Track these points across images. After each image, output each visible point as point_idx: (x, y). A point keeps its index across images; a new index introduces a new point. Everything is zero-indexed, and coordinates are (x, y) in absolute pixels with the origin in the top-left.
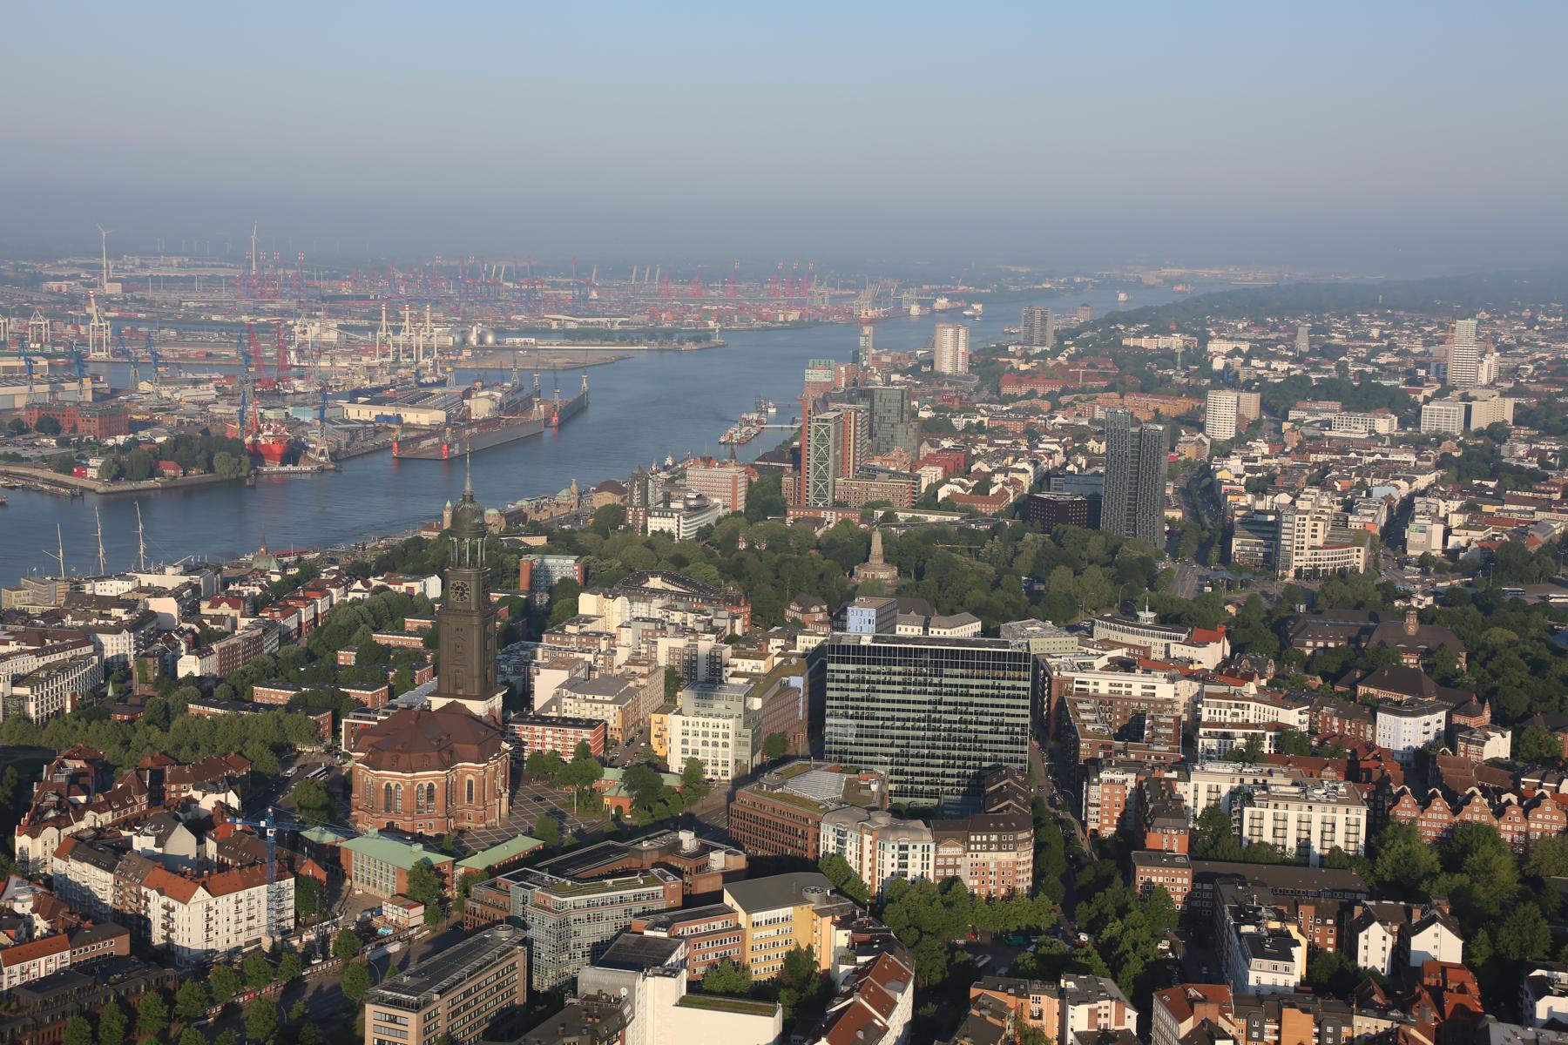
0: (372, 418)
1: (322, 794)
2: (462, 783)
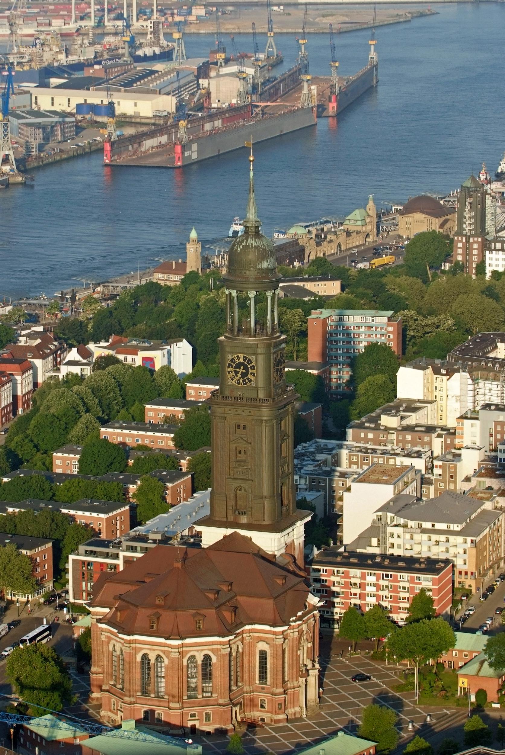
0: (72, 109)
1: (52, 668)
2: (251, 654)
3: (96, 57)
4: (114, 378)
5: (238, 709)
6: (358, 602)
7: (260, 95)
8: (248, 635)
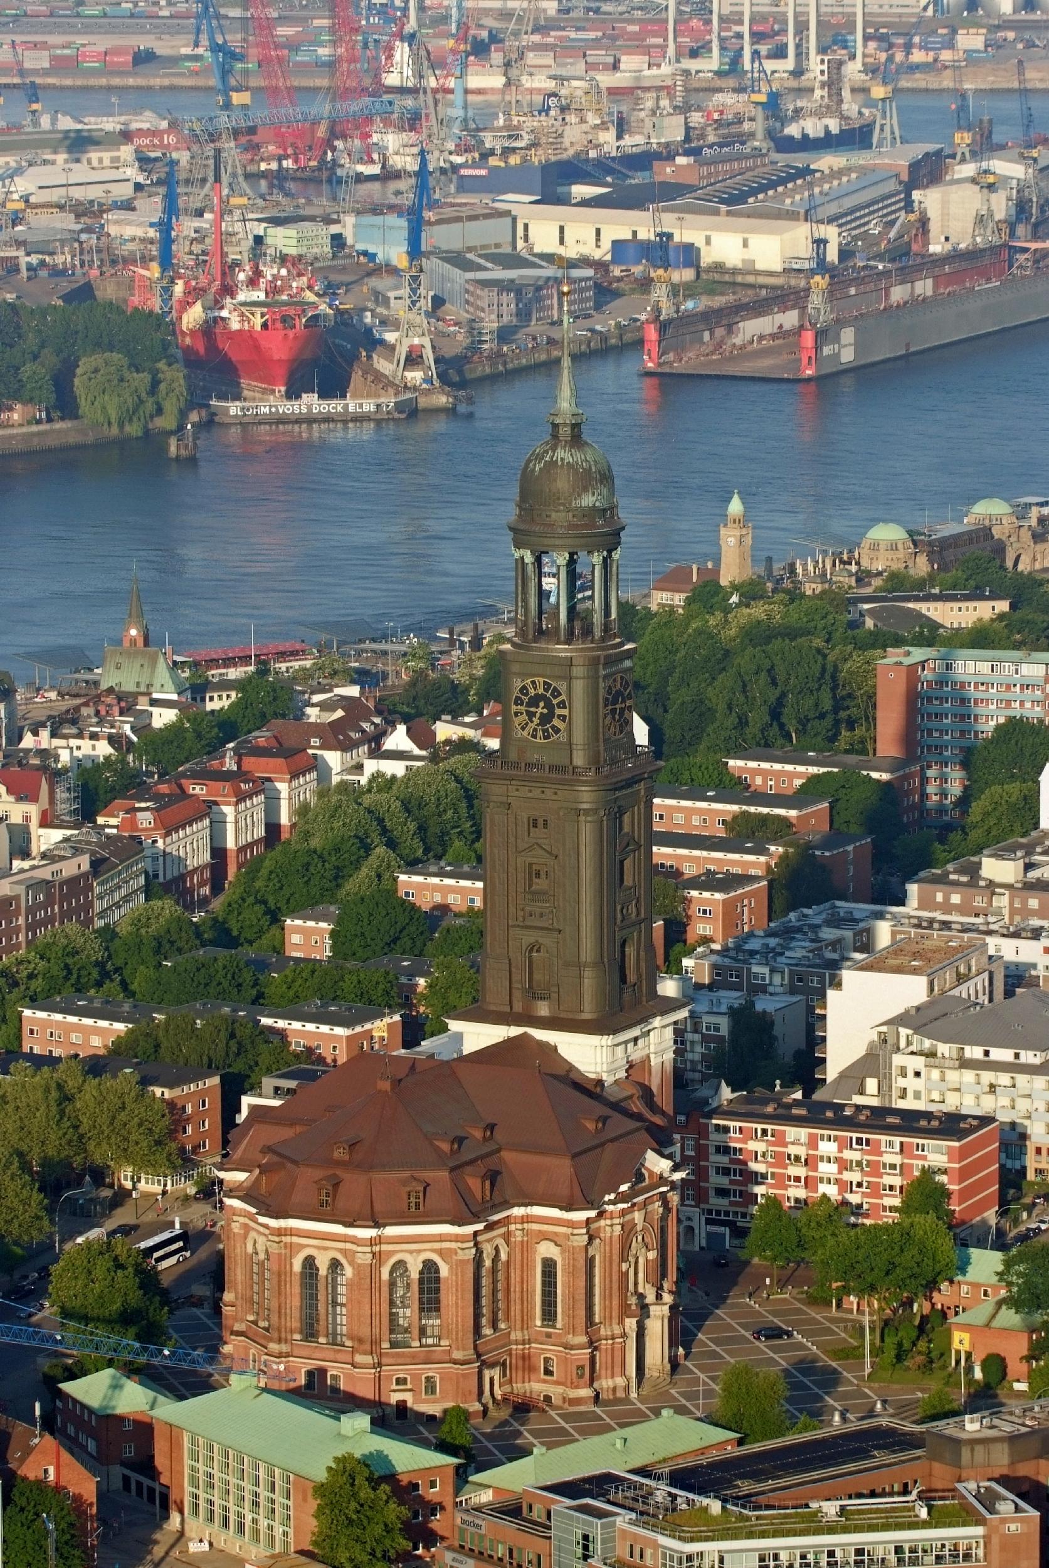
0: (603, 253)
1: (126, 1280)
2: (526, 1266)
3: (687, 139)
4: (458, 780)
5: (496, 1373)
6: (801, 1193)
7: (1036, 226)
8: (519, 1226)
